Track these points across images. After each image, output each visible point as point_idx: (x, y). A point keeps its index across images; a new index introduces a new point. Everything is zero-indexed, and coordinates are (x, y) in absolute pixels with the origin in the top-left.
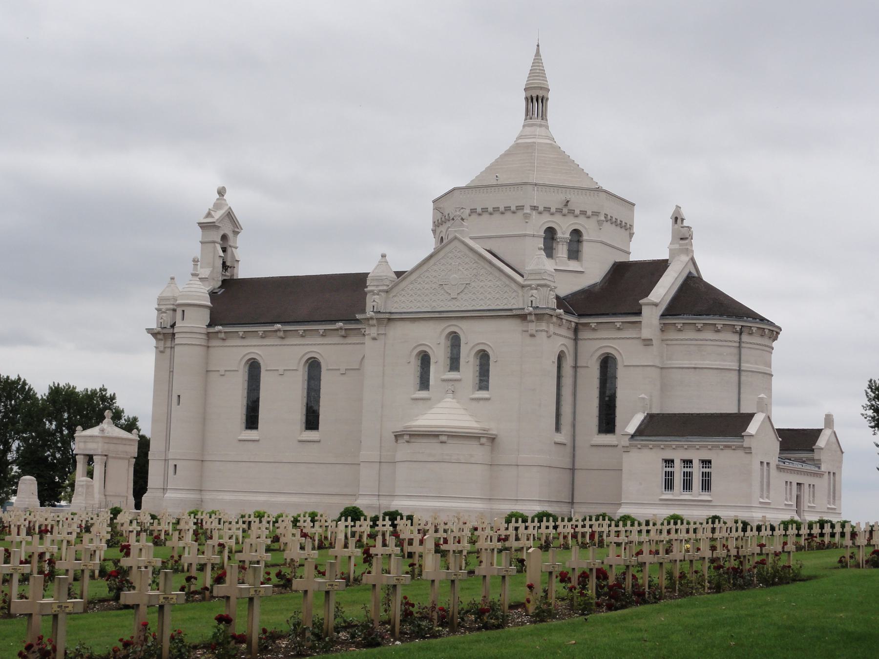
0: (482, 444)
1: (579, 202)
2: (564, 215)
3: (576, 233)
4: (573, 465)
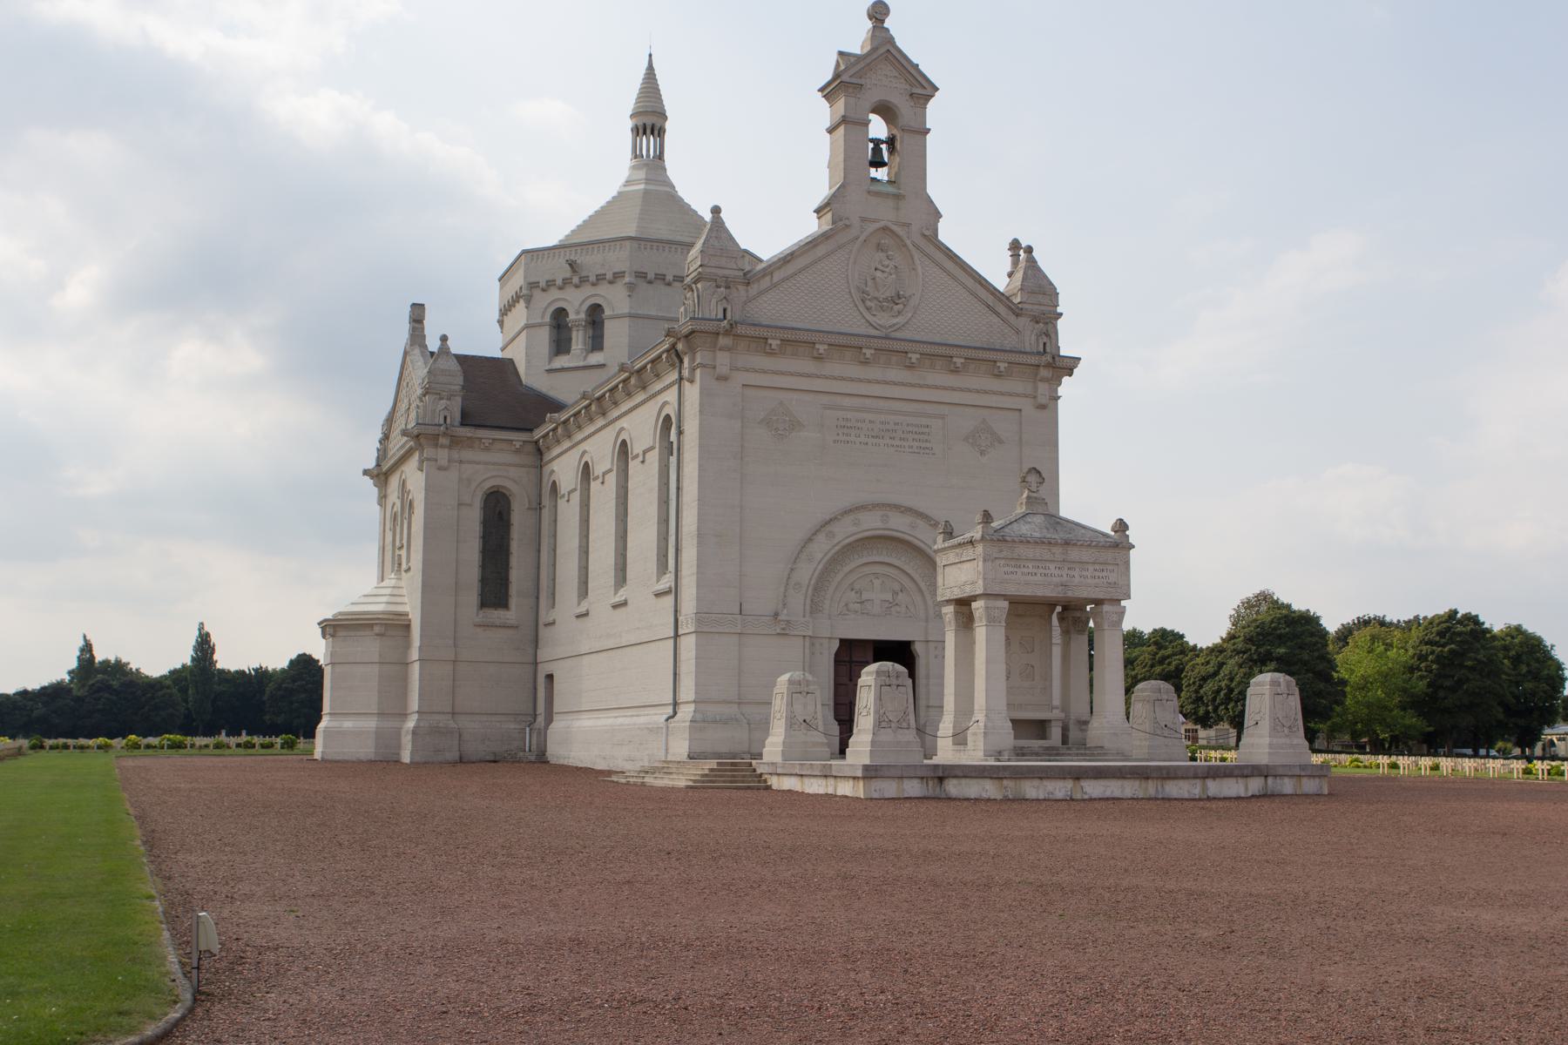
0: (377, 635)
1: (592, 262)
2: (577, 287)
3: (596, 310)
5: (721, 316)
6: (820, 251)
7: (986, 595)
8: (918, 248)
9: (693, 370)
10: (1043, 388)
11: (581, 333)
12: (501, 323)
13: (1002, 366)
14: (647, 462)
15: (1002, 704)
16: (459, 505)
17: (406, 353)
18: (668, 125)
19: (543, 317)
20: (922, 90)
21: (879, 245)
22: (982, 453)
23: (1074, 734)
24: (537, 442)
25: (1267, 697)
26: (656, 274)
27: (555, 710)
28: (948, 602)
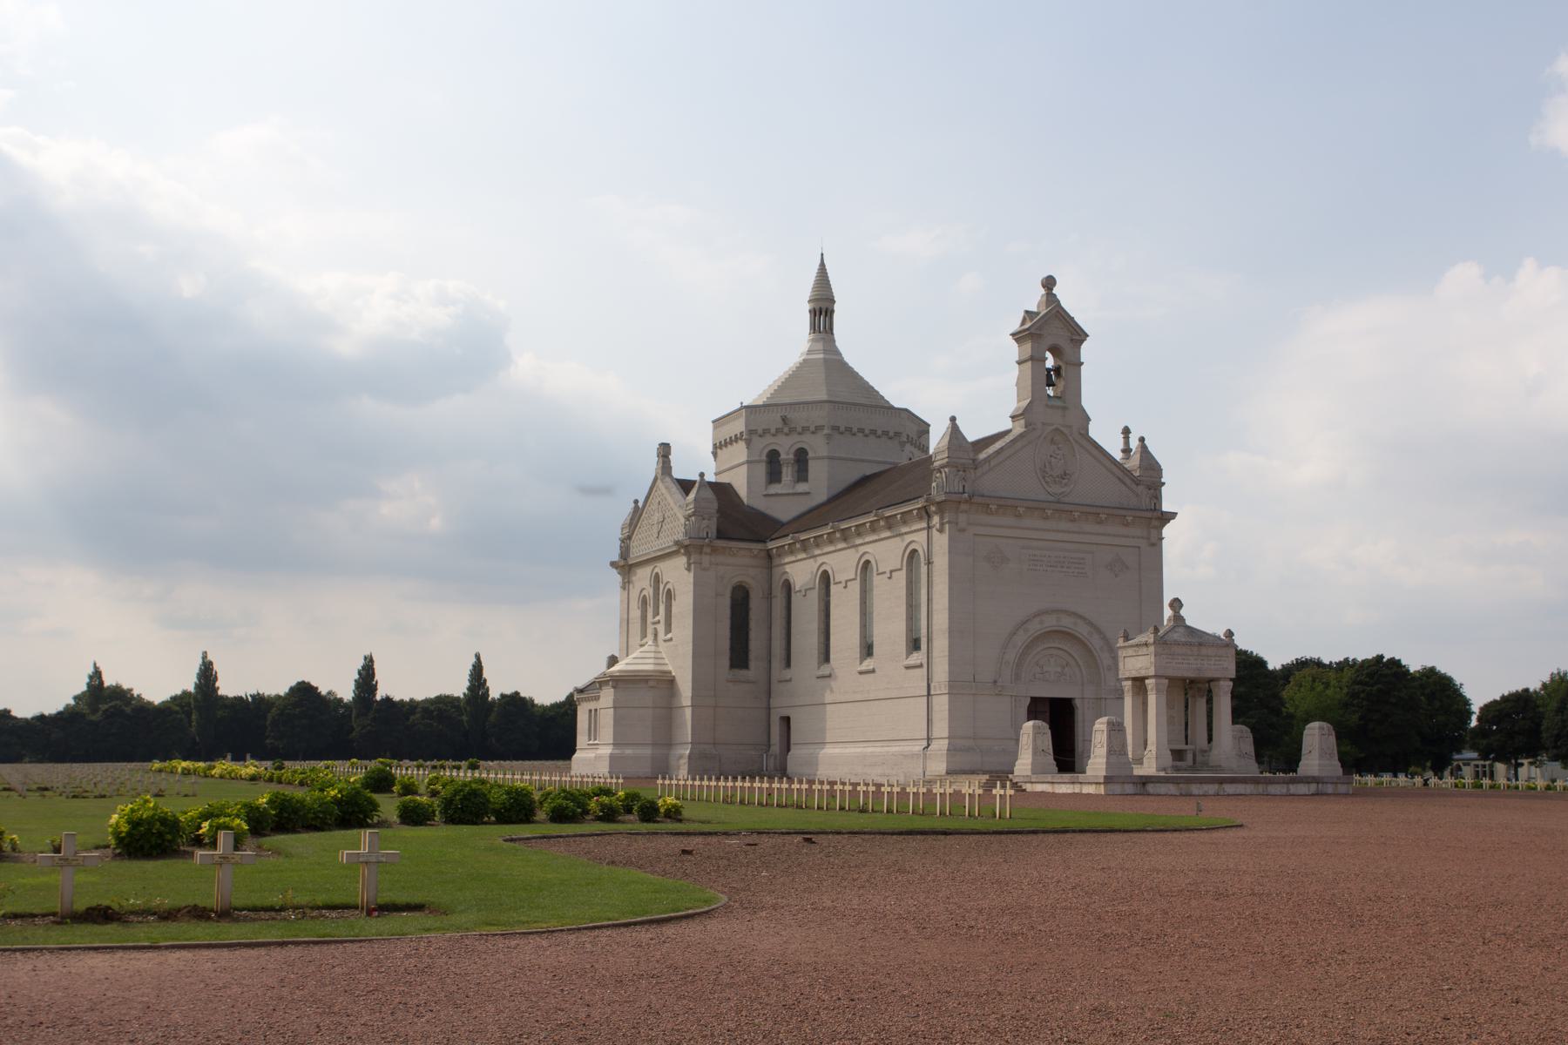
0: (652, 687)
2: (787, 435)
4: (769, 705)
5: (961, 490)
6: (1019, 445)
7: (1155, 676)
8: (1076, 442)
9: (942, 524)
10: (1154, 532)
11: (790, 469)
12: (715, 454)
13: (1130, 519)
14: (893, 578)
15: (1165, 741)
16: (717, 595)
17: (655, 480)
18: (836, 307)
19: (760, 456)
20: (1077, 335)
21: (1052, 439)
22: (1116, 576)
23: (1199, 758)
24: (768, 550)
25: (1317, 736)
26: (846, 428)
27: (792, 742)
28: (1127, 679)
